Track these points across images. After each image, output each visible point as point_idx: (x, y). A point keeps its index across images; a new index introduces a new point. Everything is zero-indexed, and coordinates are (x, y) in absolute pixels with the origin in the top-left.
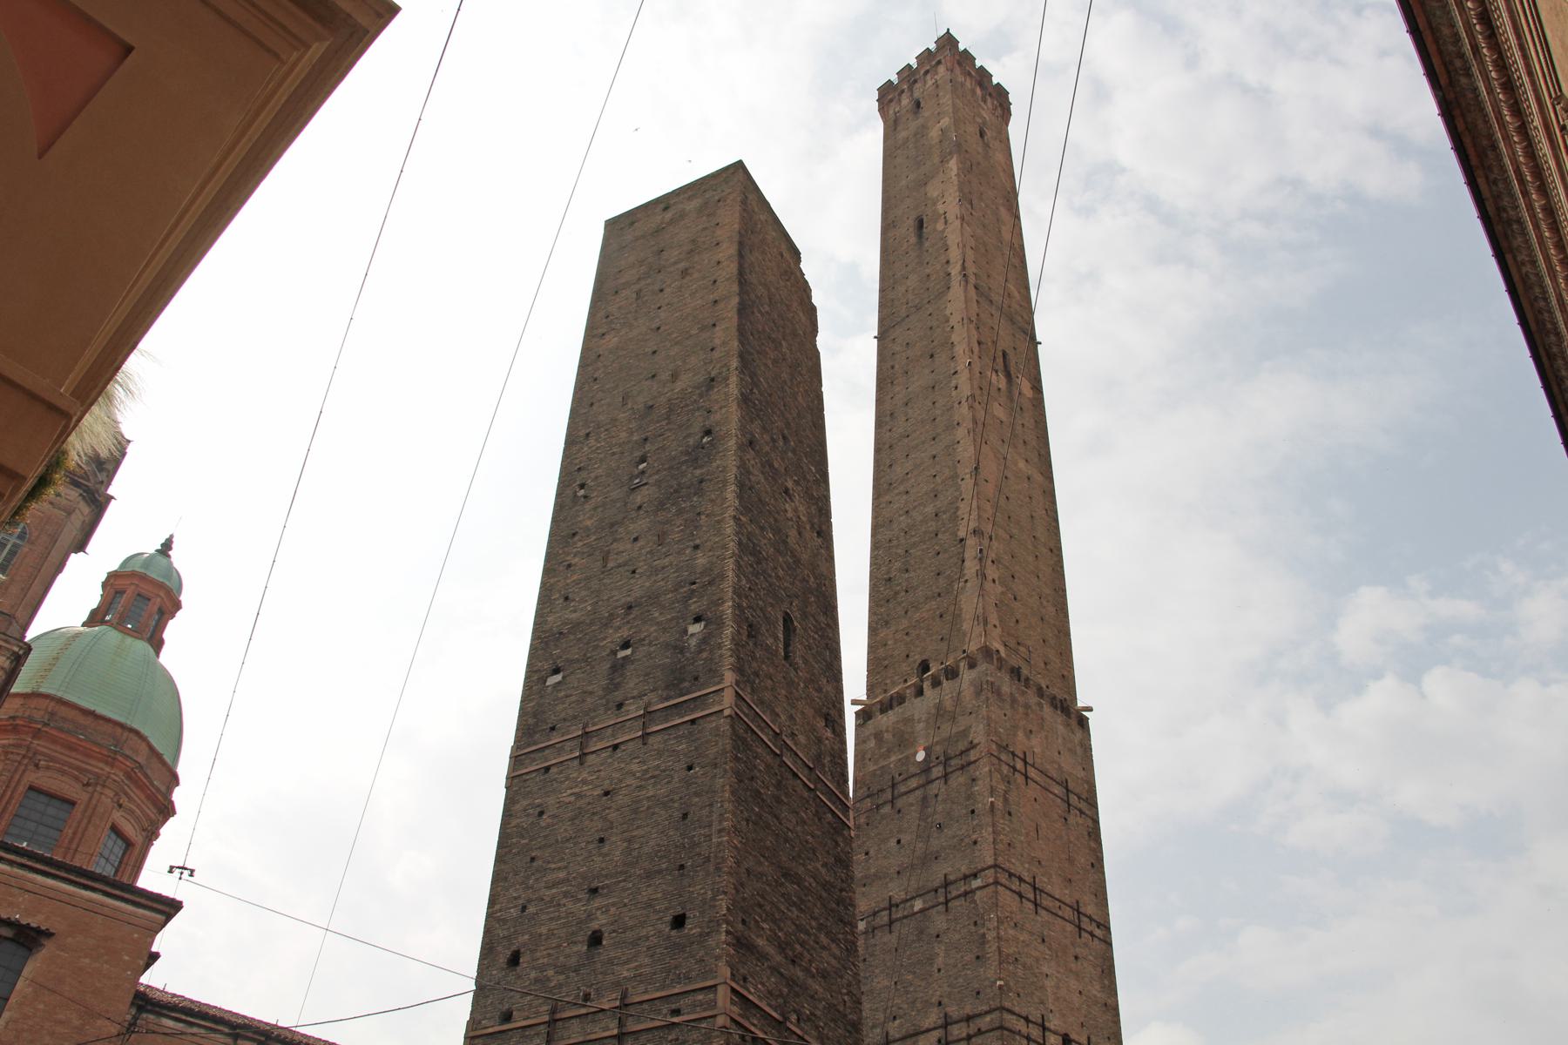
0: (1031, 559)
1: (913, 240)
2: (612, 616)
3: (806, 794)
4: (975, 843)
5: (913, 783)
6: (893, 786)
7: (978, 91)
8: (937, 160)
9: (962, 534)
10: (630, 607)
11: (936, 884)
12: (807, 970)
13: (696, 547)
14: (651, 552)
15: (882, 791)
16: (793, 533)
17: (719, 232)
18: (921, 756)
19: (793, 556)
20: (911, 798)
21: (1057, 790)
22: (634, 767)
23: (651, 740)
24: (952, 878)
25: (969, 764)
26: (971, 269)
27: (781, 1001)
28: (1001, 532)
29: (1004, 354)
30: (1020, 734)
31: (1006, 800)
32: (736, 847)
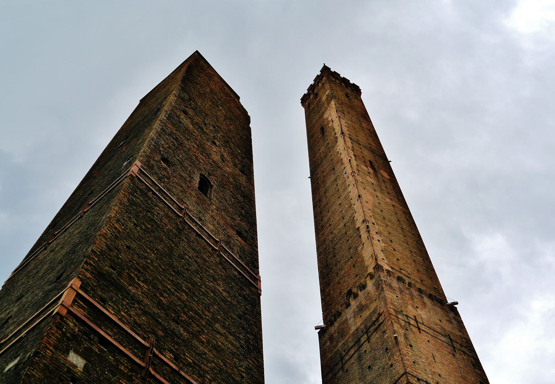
0: (401, 236)
4: (392, 366)
8: (326, 105)
9: (357, 227)
20: (353, 360)
28: (379, 222)
29: (370, 162)
30: (410, 307)
31: (406, 338)
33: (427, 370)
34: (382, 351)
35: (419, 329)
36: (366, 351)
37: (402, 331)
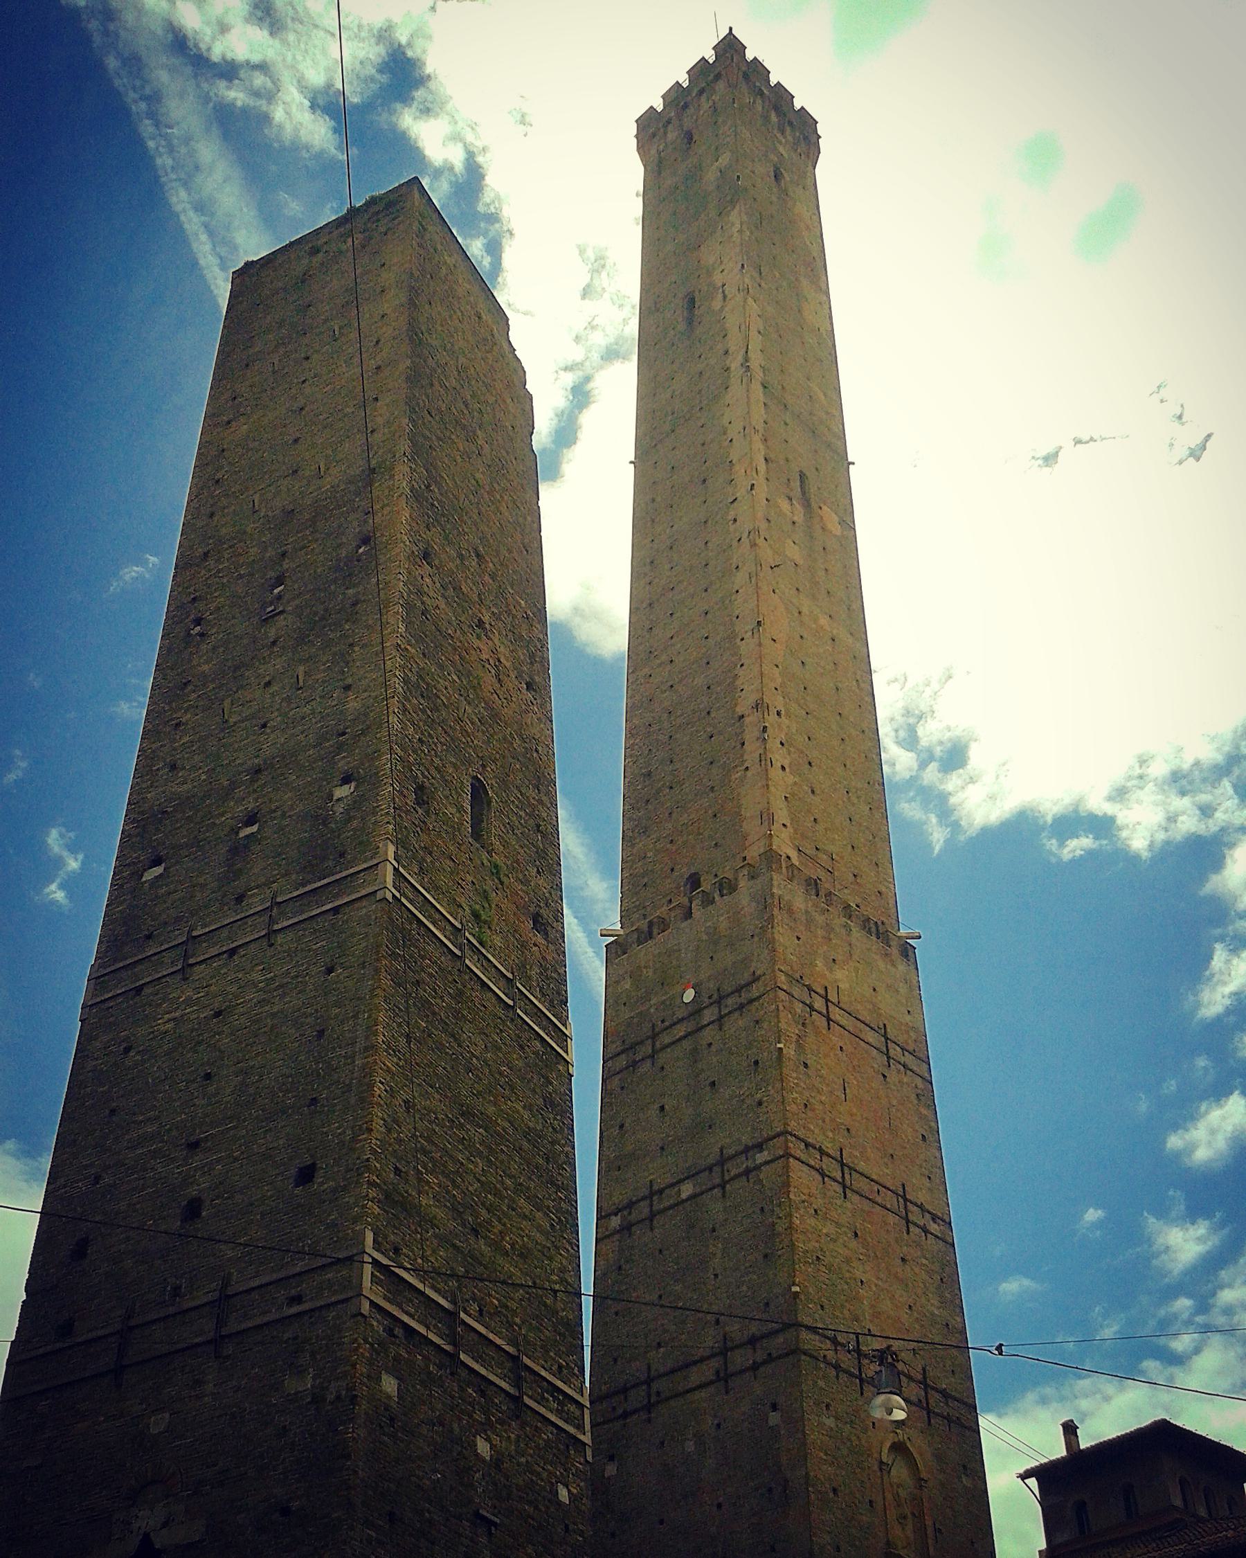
1: (682, 327)
2: (234, 785)
3: (501, 1012)
4: (760, 1103)
5: (680, 1031)
6: (654, 1037)
7: (774, 118)
10: (258, 771)
11: (710, 1161)
12: (496, 1246)
13: (347, 688)
14: (288, 699)
15: (642, 1042)
16: (489, 680)
17: (384, 275)
18: (689, 995)
19: (488, 707)
21: (871, 1037)
22: (256, 976)
23: (280, 939)
24: (731, 1151)
25: (751, 1001)
26: (756, 360)
27: (453, 1283)
29: (802, 476)
31: (800, 1046)
32: (389, 1071)
33: (827, 1119)
34: (745, 1064)
35: (829, 1019)
36: (710, 1045)
37: (795, 1030)
